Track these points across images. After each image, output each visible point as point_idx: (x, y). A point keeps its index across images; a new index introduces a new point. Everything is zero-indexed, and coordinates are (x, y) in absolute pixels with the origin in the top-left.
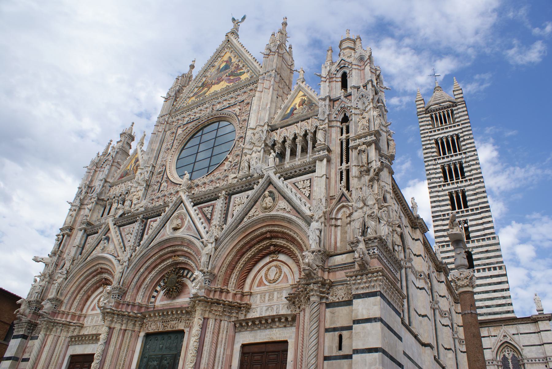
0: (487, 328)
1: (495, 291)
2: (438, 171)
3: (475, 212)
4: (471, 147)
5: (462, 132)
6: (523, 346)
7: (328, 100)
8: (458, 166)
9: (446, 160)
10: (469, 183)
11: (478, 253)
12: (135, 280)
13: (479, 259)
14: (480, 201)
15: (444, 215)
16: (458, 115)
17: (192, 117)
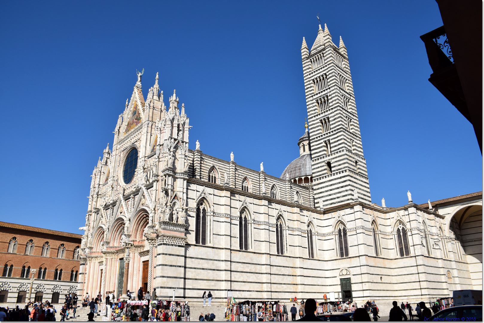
0: (330, 214)
1: (342, 187)
2: (314, 105)
3: (334, 133)
4: (333, 83)
5: (327, 72)
6: (347, 222)
7: (159, 145)
8: (326, 99)
9: (319, 95)
10: (331, 111)
11: (334, 162)
12: (112, 236)
13: (334, 167)
14: (337, 124)
15: (317, 138)
16: (326, 58)
17: (125, 146)
